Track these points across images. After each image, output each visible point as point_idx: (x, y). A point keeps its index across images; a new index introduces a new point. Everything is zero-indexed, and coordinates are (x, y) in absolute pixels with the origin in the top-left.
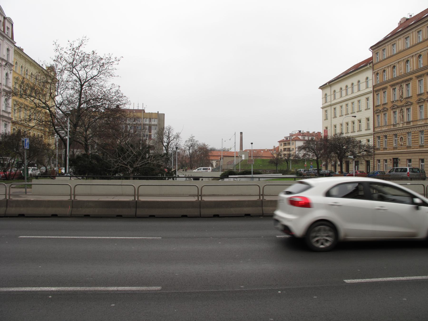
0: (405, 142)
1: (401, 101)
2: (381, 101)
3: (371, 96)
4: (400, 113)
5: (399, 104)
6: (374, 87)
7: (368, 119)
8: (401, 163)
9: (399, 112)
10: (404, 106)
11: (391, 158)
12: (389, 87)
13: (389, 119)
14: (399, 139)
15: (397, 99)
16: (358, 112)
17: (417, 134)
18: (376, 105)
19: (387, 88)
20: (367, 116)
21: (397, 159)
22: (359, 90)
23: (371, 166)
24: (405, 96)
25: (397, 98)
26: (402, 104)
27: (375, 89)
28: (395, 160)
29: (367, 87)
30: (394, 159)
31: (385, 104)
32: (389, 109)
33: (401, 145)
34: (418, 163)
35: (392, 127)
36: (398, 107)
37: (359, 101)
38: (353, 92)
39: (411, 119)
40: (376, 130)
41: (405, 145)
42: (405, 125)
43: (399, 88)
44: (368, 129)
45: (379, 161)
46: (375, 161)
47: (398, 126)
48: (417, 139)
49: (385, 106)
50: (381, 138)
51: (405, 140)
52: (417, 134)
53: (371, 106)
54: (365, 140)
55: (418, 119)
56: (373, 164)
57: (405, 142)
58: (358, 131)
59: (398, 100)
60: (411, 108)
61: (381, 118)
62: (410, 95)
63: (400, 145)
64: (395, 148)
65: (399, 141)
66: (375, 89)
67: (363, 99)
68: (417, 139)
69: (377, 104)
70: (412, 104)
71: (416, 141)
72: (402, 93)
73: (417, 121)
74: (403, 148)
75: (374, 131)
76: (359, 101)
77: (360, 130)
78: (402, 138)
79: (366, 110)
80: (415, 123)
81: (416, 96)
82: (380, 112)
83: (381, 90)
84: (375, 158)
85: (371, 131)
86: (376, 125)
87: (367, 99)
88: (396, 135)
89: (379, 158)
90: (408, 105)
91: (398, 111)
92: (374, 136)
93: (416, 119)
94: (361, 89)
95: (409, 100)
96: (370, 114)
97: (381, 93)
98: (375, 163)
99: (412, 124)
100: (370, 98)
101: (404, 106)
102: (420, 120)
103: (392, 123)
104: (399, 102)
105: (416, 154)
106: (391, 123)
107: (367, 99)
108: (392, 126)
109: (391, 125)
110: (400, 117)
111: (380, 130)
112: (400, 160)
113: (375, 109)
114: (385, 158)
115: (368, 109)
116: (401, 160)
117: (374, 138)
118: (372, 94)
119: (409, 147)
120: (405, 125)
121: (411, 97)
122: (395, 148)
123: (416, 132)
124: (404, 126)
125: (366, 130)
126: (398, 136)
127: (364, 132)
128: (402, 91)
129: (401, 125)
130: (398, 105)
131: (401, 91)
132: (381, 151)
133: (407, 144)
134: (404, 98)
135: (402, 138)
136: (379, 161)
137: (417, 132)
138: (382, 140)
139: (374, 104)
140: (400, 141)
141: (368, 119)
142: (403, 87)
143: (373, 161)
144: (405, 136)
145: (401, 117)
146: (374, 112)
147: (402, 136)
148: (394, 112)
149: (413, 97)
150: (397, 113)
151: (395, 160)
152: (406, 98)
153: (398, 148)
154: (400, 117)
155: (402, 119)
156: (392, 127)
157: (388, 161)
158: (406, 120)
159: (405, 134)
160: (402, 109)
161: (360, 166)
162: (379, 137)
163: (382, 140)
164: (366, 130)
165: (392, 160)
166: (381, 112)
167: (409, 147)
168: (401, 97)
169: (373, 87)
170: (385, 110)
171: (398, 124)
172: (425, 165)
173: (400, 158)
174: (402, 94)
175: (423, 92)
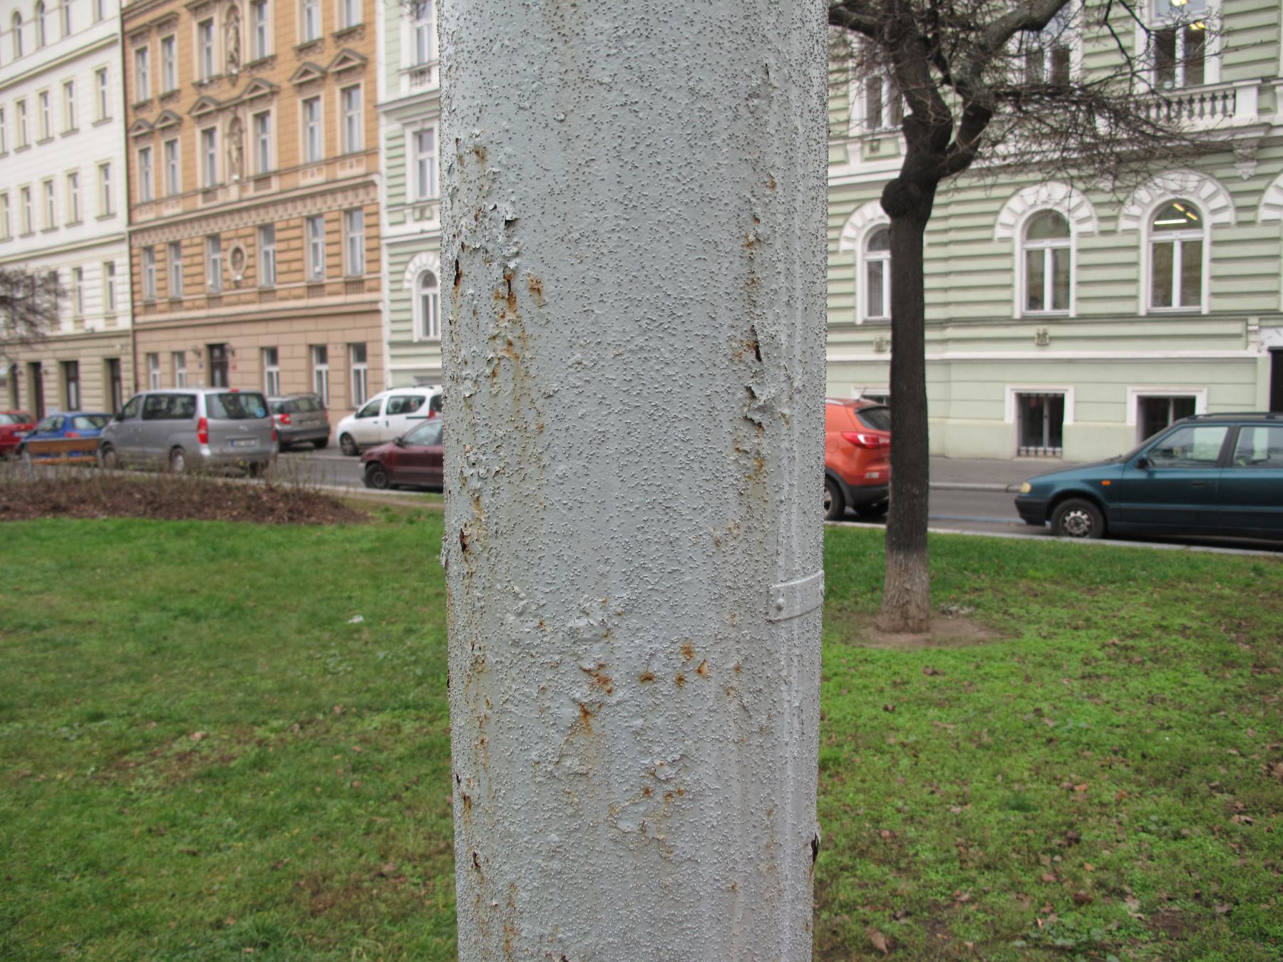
0: (250, 272)
1: (233, 79)
2: (155, 83)
3: (113, 59)
4: (231, 135)
5: (224, 93)
6: (126, 15)
7: (104, 167)
8: (241, 366)
9: (227, 130)
10: (243, 103)
11: (201, 345)
12: (185, 15)
13: (189, 168)
14: (228, 255)
15: (216, 70)
16: (65, 135)
17: (296, 233)
18: (134, 100)
19: (176, 19)
20: (102, 157)
21: (221, 347)
22: (67, 33)
23: (125, 384)
24: (246, 57)
25: (218, 67)
26: (235, 93)
27: (129, 27)
28: (217, 353)
29: (100, 17)
30: (211, 347)
31: (170, 96)
32: (186, 118)
33: (237, 284)
34: (302, 364)
35: (199, 202)
36: (221, 110)
37: (68, 85)
38: (42, 44)
39: (273, 165)
40: (142, 217)
41: (250, 282)
42: (251, 191)
43: (224, 20)
44: (108, 215)
45: (154, 357)
46: (141, 358)
47: (221, 197)
48: (297, 255)
49: (171, 106)
50: (158, 256)
51: (251, 262)
52: (296, 233)
53: (117, 110)
54: (98, 264)
55: (301, 161)
56: (131, 375)
57: (250, 272)
58: (69, 225)
59: (219, 77)
60: (273, 109)
61: (158, 160)
62: (269, 51)
63: (233, 286)
64: (214, 300)
65: (229, 265)
66: (130, 26)
67: (83, 73)
68: (297, 255)
69: (138, 97)
70: (275, 92)
71: (295, 266)
72: (238, 40)
73: (295, 170)
74: (243, 298)
75: (130, 222)
76: (68, 85)
77: (76, 223)
78: (237, 250)
79: (96, 124)
80: (289, 181)
81: (292, 55)
82: (150, 135)
83: (154, 31)
84: (141, 348)
85: (119, 225)
86: (138, 197)
87: (101, 73)
88: (215, 238)
89: (151, 348)
90: (261, 95)
91: (221, 125)
92: (131, 248)
93: (291, 164)
94: (75, 29)
95: (264, 74)
96: (111, 143)
97: (154, 43)
98: (142, 369)
99: (275, 185)
100: (108, 75)
101: (243, 103)
102: (306, 166)
103: (200, 185)
104: (226, 85)
105: (298, 325)
106: (195, 182)
107: (101, 73)
108: (200, 198)
109: (196, 192)
110: (229, 153)
111: (151, 216)
112: (233, 353)
113: (132, 120)
114: (178, 347)
115: (105, 120)
116: (238, 352)
117: (131, 257)
118: (117, 51)
119: (266, 293)
120: (251, 191)
121: (273, 58)
122: (214, 300)
123: (292, 223)
124: (245, 195)
125: (101, 218)
126: (224, 245)
127: (92, 229)
128: (237, 32)
129: (234, 193)
130: (223, 97)
131: (232, 32)
132: (162, 312)
133: (262, 281)
134: (246, 67)
135: (237, 250)
136: (154, 357)
137: (297, 222)
138: (161, 265)
139: (129, 97)
140: (234, 264)
141: (104, 167)
142: (240, 15)
143: (130, 358)
144: (250, 241)
145: (235, 154)
146: (127, 131)
147: (242, 246)
148: (209, 133)
149: (281, 59)
150: (218, 135)
151: (217, 353)
152: (255, 65)
153: (225, 300)
154: (229, 153)
155: (237, 166)
156: (199, 202)
157: (190, 356)
158: (251, 169)
159: (249, 231)
160: (236, 120)
161: (83, 384)
162: (149, 249)
163: (161, 265)
164: (101, 218)
165: (205, 355)
166: (157, 134)
167: (266, 293)
168: (233, 60)
169: (122, 15)
170: (170, 125)
171: (223, 186)
172: (331, 374)
173: (233, 343)
174: (237, 50)
175: (317, 33)
